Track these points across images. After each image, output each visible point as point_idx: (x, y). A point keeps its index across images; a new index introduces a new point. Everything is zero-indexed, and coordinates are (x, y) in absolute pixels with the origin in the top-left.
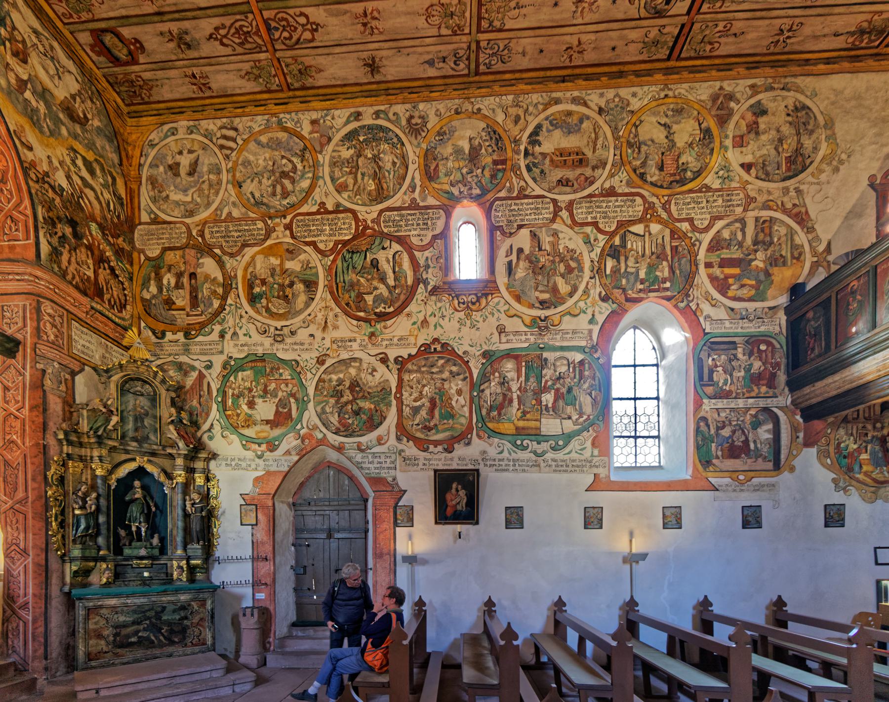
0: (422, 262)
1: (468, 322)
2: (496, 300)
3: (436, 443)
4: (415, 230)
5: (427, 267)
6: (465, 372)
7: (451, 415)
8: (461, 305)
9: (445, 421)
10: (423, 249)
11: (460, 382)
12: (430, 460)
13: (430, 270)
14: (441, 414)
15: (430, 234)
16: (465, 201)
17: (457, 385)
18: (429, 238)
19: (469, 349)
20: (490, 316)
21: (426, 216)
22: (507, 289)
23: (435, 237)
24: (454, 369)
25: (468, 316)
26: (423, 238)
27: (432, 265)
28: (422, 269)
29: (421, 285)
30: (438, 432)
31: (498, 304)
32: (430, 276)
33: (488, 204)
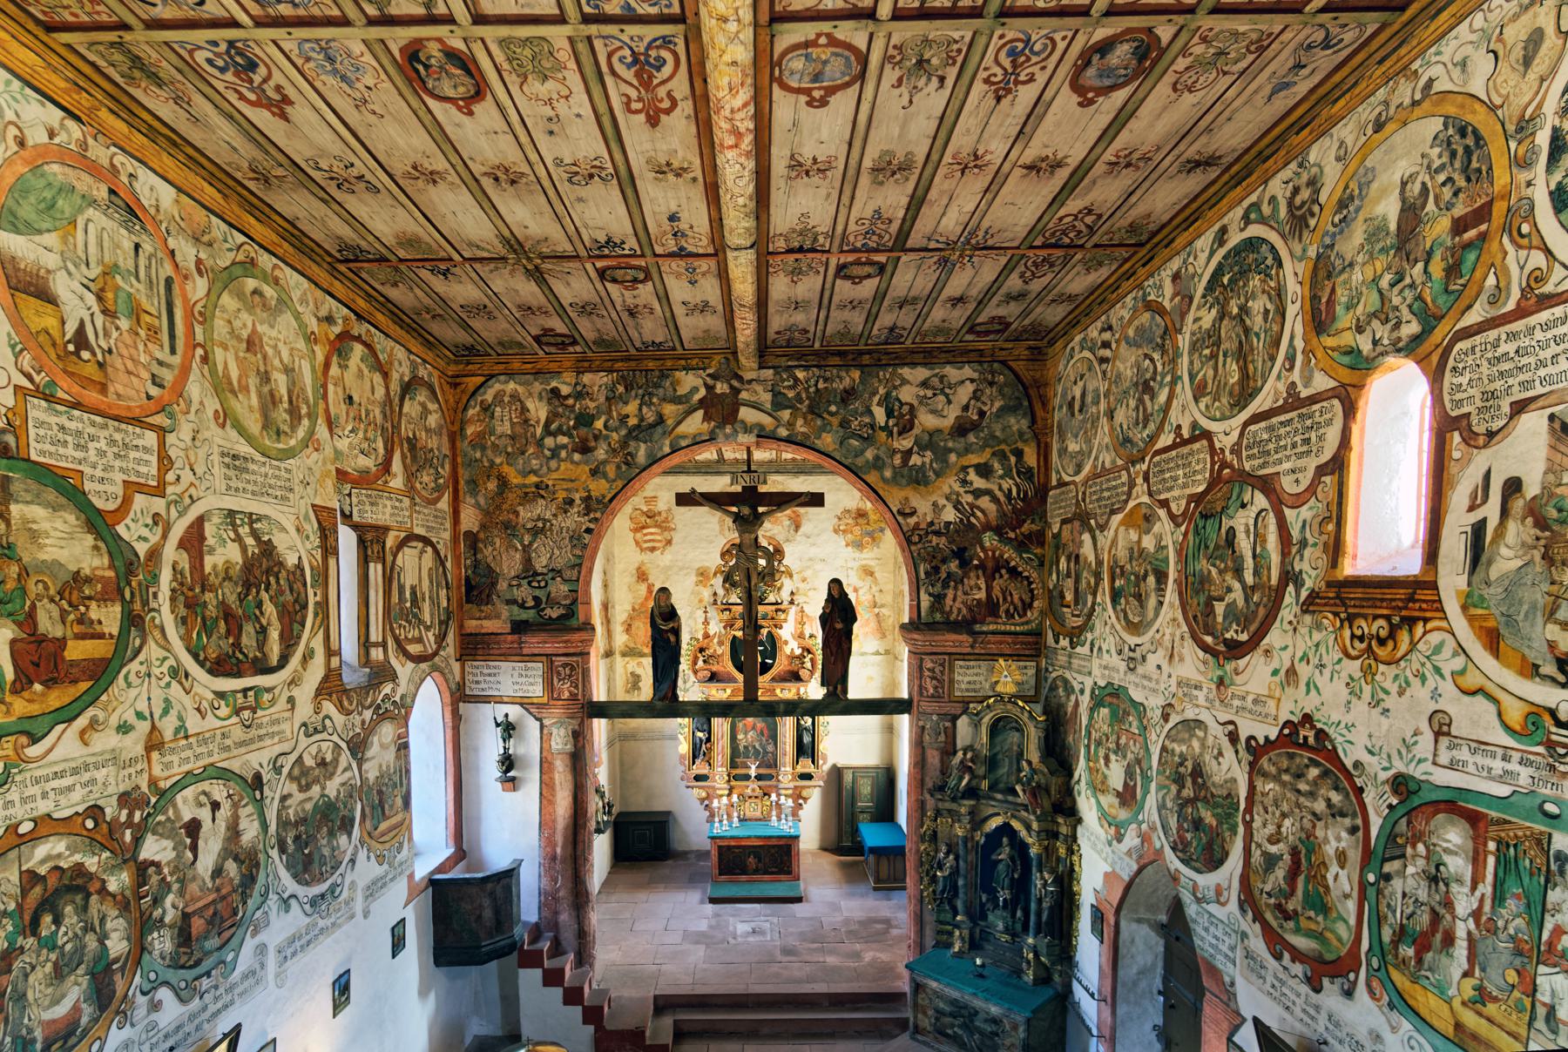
0: (1295, 533)
1: (1367, 689)
2: (1435, 638)
3: (1297, 956)
4: (1288, 458)
5: (1303, 543)
6: (1354, 816)
7: (1320, 903)
8: (1357, 644)
9: (1312, 914)
10: (1299, 501)
11: (1344, 835)
12: (1283, 983)
13: (1307, 552)
14: (1306, 893)
15: (1312, 463)
16: (1391, 360)
17: (1339, 839)
18: (1310, 473)
19: (1365, 758)
20: (1416, 682)
21: (1308, 423)
22: (1464, 608)
23: (1321, 471)
24: (1336, 798)
25: (1368, 673)
26: (1300, 476)
27: (1311, 540)
28: (1294, 550)
29: (1291, 588)
30: (1297, 931)
31: (1438, 649)
32: (1305, 566)
33: (1435, 358)
